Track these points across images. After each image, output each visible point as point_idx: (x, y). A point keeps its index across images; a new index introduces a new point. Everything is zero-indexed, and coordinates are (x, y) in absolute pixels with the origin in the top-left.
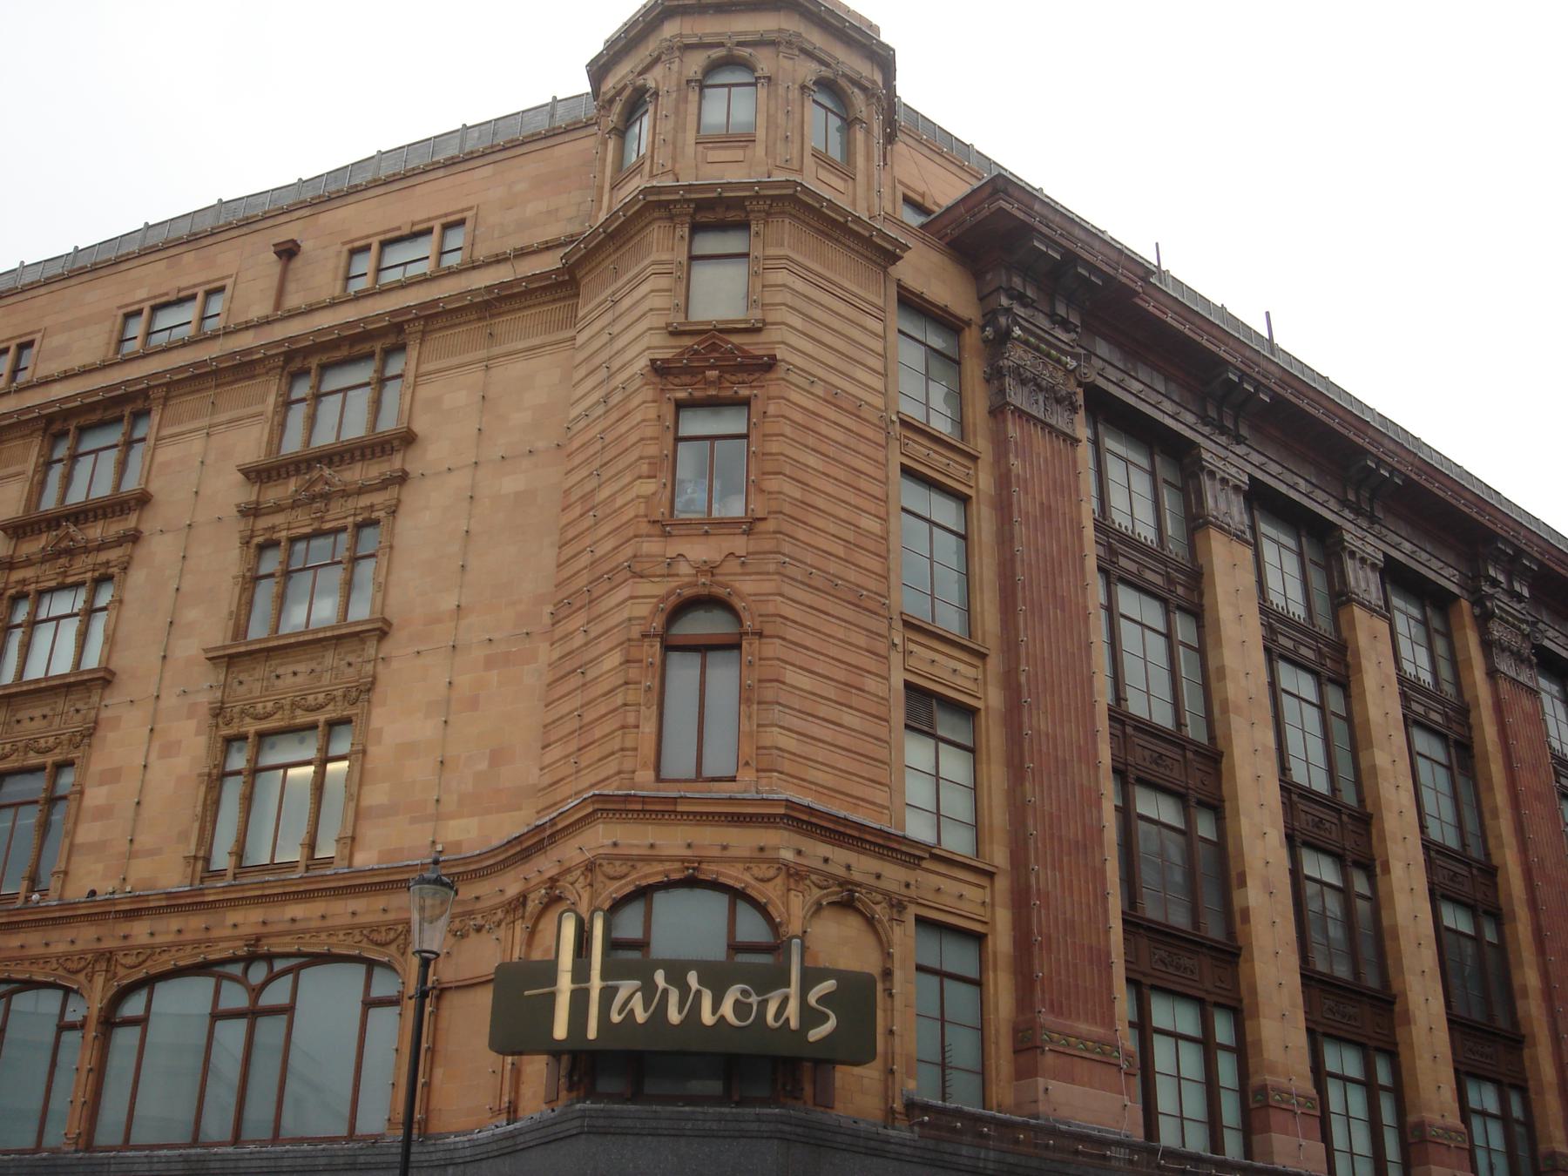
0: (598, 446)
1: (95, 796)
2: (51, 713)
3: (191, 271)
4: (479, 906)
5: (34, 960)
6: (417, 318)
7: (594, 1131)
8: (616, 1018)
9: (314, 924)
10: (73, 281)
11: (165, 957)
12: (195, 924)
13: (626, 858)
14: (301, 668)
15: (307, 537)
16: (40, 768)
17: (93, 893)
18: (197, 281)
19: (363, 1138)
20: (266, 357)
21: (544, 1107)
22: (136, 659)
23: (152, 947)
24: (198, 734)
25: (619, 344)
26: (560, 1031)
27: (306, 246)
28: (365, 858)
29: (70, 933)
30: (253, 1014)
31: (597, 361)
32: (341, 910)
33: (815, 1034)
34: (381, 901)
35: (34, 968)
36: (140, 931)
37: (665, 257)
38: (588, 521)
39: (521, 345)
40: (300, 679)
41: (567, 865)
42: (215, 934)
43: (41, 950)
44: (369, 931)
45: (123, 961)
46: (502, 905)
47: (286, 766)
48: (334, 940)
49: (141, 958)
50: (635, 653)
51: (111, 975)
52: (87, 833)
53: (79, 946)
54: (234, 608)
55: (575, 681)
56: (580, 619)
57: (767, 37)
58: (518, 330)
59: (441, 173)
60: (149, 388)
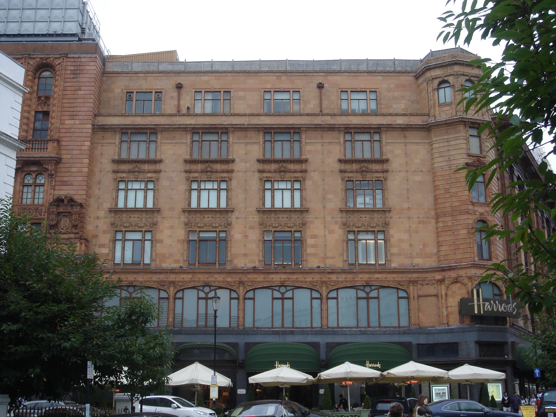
0: (449, 178)
1: (310, 241)
2: (289, 217)
3: (285, 84)
4: (426, 279)
5: (301, 282)
6: (385, 127)
7: (479, 330)
8: (486, 310)
9: (384, 279)
10: (241, 74)
11: (342, 284)
12: (350, 277)
13: (477, 276)
14: (367, 216)
15: (360, 181)
16: (291, 231)
17: (319, 267)
18: (290, 87)
19: (403, 327)
20: (340, 127)
21: (459, 324)
22: (314, 205)
23: (338, 281)
24: (339, 229)
25: (452, 153)
26: (476, 312)
27: (326, 85)
28: (394, 265)
29: (312, 276)
30: (368, 298)
31: (443, 155)
32: (391, 277)
33: (514, 313)
34: (400, 275)
35: (302, 284)
36: (334, 277)
37: (464, 135)
38: (448, 195)
39: (414, 141)
40: (367, 219)
41: (460, 275)
42: (356, 279)
43: (303, 280)
44: (399, 282)
45: (330, 284)
46: (434, 280)
47: (366, 240)
48: (389, 283)
49: (335, 284)
50: (471, 231)
51: (327, 287)
52: (310, 250)
53: (315, 279)
54: (344, 197)
55: (449, 233)
56: (449, 219)
57: (478, 76)
58: (413, 137)
59: (366, 74)
60: (301, 127)
